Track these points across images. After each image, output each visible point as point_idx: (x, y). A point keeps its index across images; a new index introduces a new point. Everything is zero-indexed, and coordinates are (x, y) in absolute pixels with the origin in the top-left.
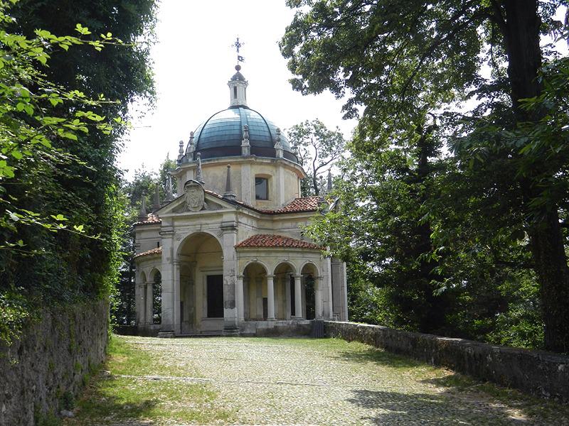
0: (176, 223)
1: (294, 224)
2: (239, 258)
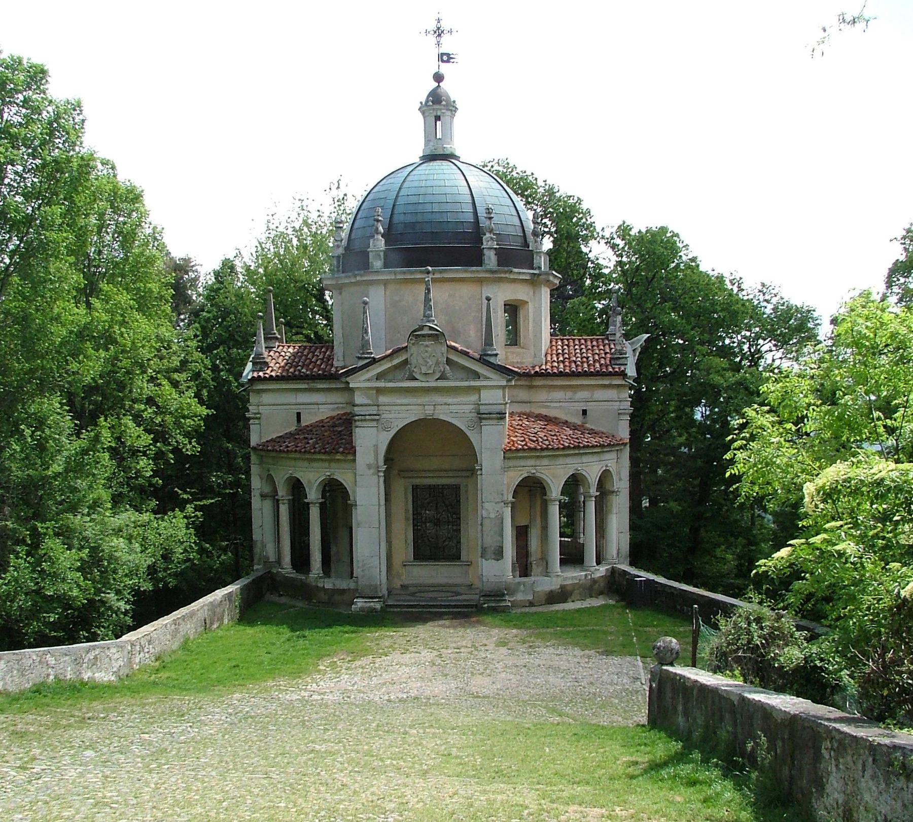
0: (383, 399)
1: (569, 394)
2: (505, 469)
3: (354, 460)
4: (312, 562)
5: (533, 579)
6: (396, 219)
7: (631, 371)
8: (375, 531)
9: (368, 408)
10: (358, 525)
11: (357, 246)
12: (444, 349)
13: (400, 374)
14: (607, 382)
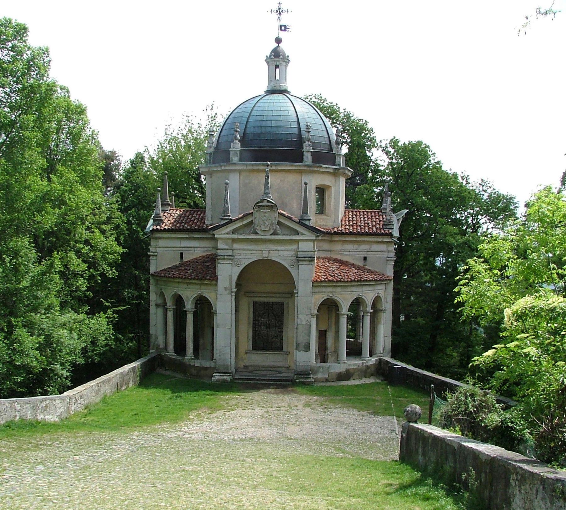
0: (236, 246)
1: (356, 246)
2: (313, 293)
3: (216, 285)
4: (187, 349)
5: (328, 364)
6: (248, 131)
7: (396, 233)
8: (228, 331)
9: (227, 251)
10: (218, 326)
11: (223, 147)
12: (277, 215)
13: (247, 230)
14: (380, 240)
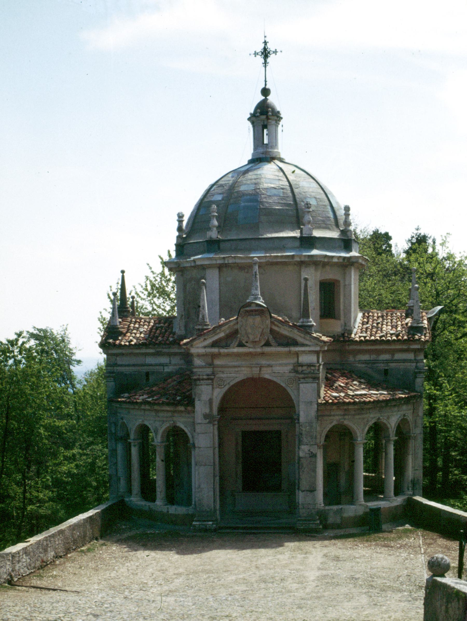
0: (217, 362)
